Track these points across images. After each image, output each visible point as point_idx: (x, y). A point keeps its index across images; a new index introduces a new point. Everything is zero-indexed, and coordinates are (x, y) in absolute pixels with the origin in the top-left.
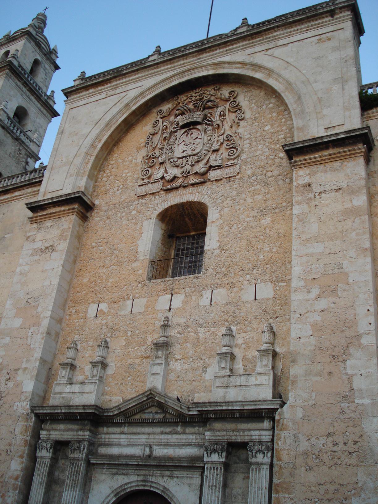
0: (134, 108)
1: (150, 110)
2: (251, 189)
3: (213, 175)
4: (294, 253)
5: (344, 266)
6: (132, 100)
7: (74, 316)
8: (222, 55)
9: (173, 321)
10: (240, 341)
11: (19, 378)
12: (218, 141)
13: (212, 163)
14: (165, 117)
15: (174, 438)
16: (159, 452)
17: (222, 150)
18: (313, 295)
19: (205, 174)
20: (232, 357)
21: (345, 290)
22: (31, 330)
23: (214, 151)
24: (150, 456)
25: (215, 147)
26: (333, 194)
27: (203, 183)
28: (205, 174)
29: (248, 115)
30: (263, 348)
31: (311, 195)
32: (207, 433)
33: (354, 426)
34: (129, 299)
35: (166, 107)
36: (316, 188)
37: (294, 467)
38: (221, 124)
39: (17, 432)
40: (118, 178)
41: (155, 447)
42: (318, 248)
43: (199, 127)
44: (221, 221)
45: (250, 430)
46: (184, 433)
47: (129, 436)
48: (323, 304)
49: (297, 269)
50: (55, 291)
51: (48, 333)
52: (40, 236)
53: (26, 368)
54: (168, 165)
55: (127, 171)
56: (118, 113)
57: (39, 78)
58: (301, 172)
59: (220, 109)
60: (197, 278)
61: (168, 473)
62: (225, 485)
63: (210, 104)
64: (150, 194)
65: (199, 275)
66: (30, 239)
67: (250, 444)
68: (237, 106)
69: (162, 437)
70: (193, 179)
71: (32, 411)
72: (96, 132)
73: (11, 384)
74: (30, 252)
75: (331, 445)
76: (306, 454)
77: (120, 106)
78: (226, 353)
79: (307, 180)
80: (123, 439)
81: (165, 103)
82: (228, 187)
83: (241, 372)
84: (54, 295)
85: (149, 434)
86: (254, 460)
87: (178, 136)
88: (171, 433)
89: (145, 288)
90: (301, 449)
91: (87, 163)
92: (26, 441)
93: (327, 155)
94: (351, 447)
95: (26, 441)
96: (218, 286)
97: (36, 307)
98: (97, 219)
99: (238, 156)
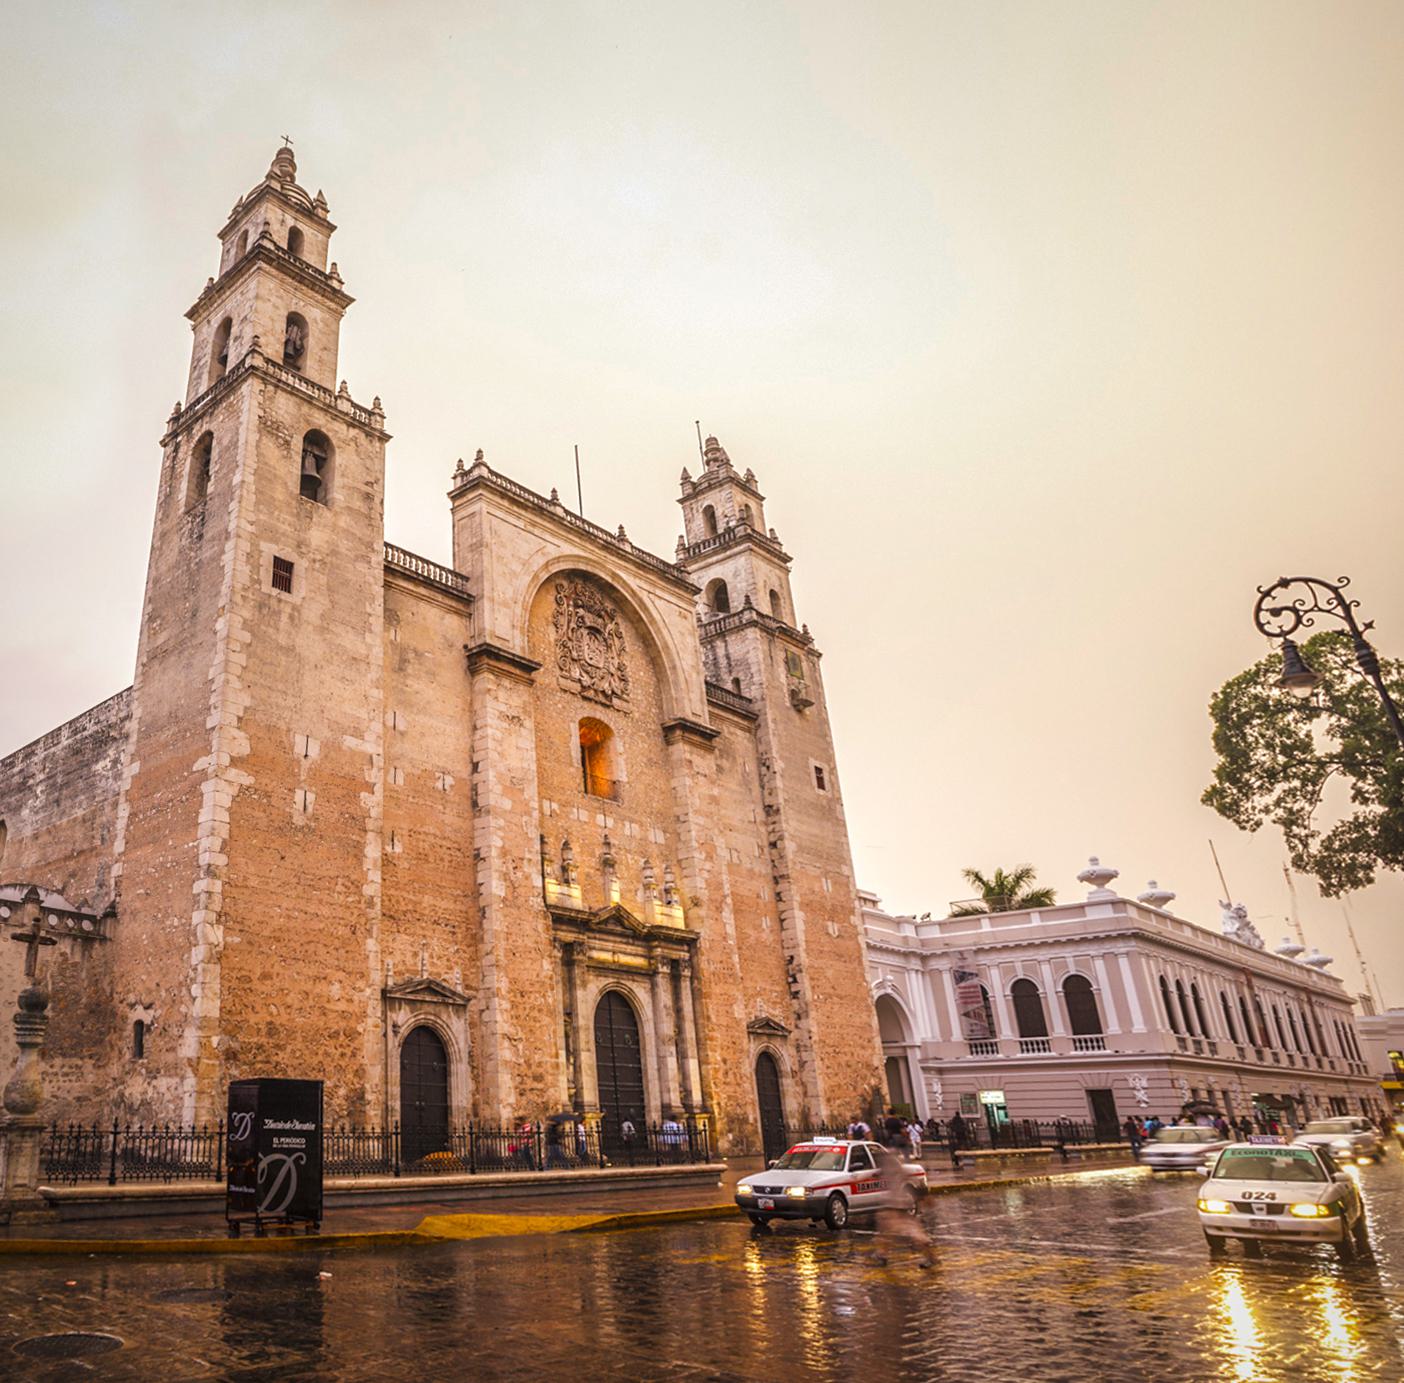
3: (616, 701)
8: (620, 567)
9: (612, 841)
15: (629, 949)
16: (624, 959)
22: (525, 818)
25: (613, 670)
27: (608, 707)
42: (702, 821)
48: (708, 866)
52: (502, 695)
53: (530, 860)
73: (519, 874)
79: (688, 756)
80: (597, 943)
97: (522, 791)
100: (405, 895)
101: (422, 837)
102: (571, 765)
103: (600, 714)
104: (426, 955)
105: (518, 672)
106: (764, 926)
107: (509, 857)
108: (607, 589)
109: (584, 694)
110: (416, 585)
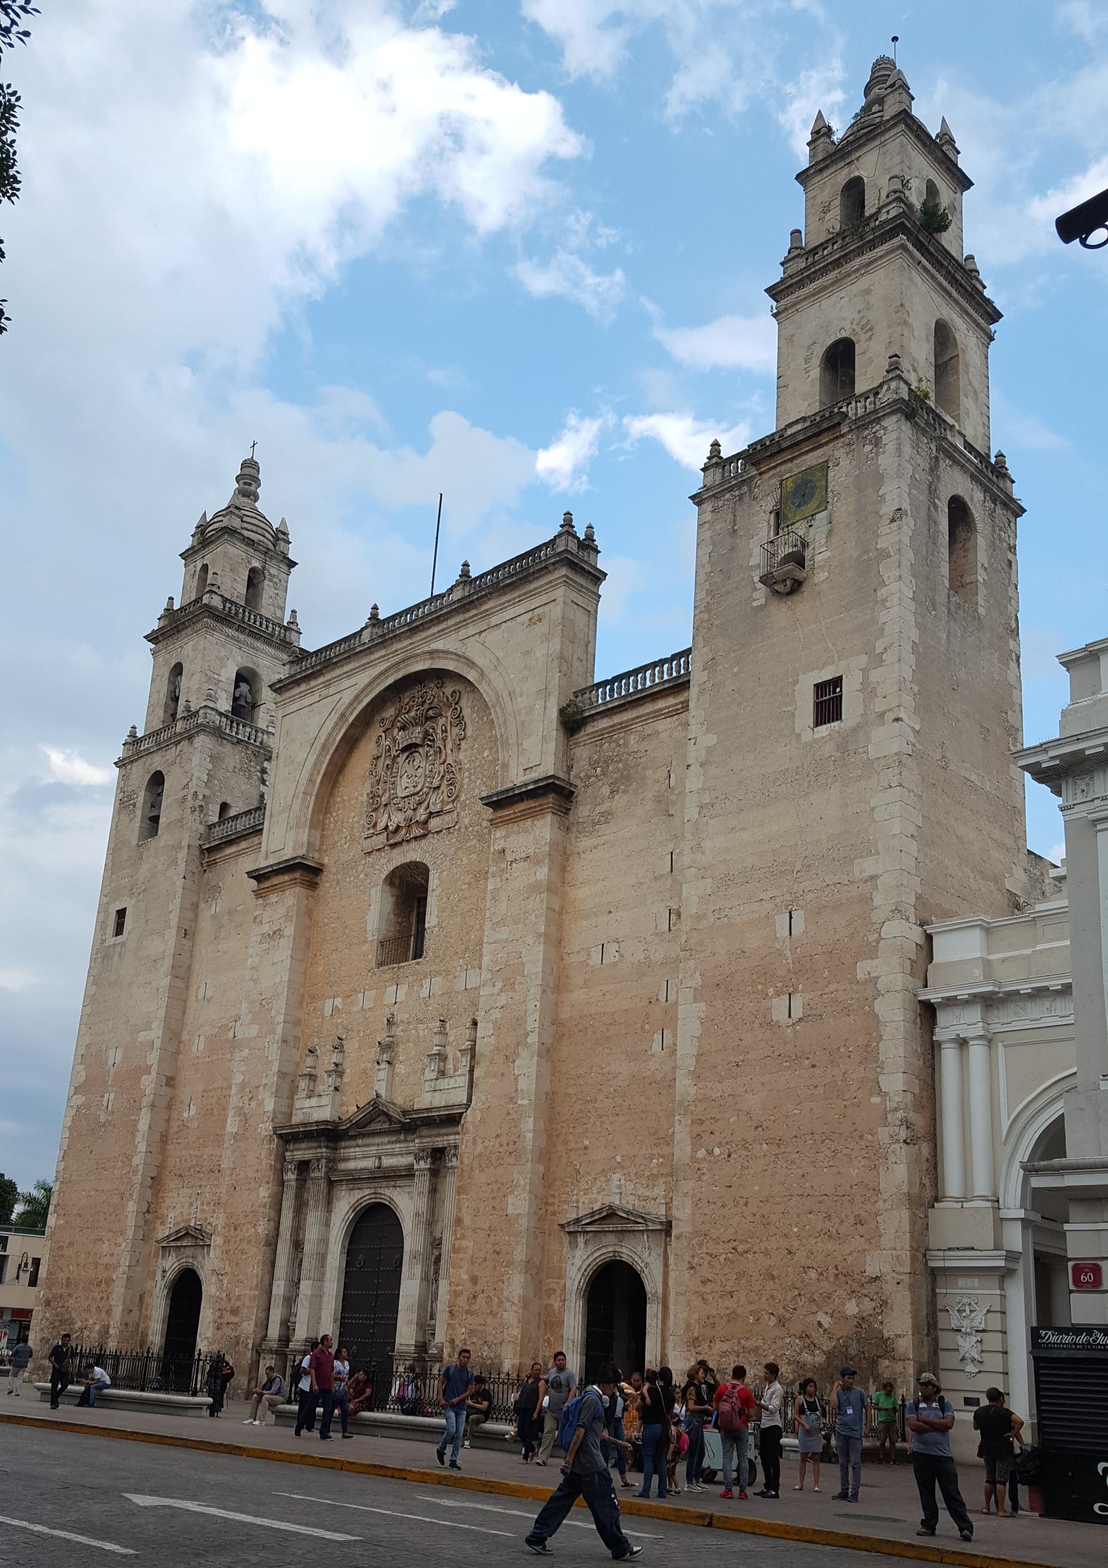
0: (351, 719)
1: (373, 716)
2: (468, 845)
3: (434, 823)
4: (485, 941)
5: (523, 955)
6: (347, 708)
7: (313, 1015)
10: (451, 1038)
11: (260, 1097)
12: (439, 772)
13: (432, 809)
14: (388, 729)
16: (387, 1162)
17: (443, 788)
18: (496, 990)
19: (426, 822)
20: (442, 1057)
21: (521, 983)
23: (435, 788)
24: (379, 1168)
25: (436, 783)
26: (522, 865)
27: (424, 836)
28: (426, 822)
29: (469, 732)
30: (463, 1048)
31: (503, 866)
32: (417, 1141)
33: (515, 1127)
34: (360, 992)
35: (390, 713)
36: (509, 857)
37: (472, 1170)
38: (442, 747)
39: (263, 1157)
40: (345, 825)
41: (383, 1157)
43: (420, 750)
44: (439, 890)
45: (448, 1135)
46: (406, 1141)
47: (363, 1149)
49: (486, 960)
50: (286, 989)
51: (284, 1041)
53: (266, 1084)
54: (392, 808)
55: (353, 814)
56: (333, 729)
57: (266, 608)
58: (498, 834)
59: (441, 721)
60: (418, 963)
61: (393, 1183)
62: (434, 1191)
63: (430, 713)
64: (377, 850)
65: (420, 960)
66: (257, 920)
67: (448, 1149)
68: (459, 717)
69: (388, 1147)
70: (417, 831)
71: (275, 1133)
72: (312, 759)
73: (253, 1104)
74: (259, 938)
75: (498, 1145)
76: (480, 1155)
77: (335, 717)
78: (435, 1055)
81: (389, 704)
82: (448, 843)
83: (451, 1072)
84: (285, 994)
85: (378, 1145)
86: (449, 1165)
87: (401, 763)
88: (396, 1142)
89: (375, 977)
90: (477, 1152)
91: (307, 808)
92: (271, 1165)
93: (519, 812)
94: (511, 1148)
95: (271, 1165)
96: (438, 973)
97: (269, 1010)
98: (327, 885)
99: (457, 796)
100: (191, 1152)
101: (210, 1094)
102: (365, 942)
103: (411, 853)
104: (199, 1203)
105: (286, 878)
106: (656, 1047)
107: (247, 1090)
108: (440, 676)
109: (395, 838)
110: (239, 843)
